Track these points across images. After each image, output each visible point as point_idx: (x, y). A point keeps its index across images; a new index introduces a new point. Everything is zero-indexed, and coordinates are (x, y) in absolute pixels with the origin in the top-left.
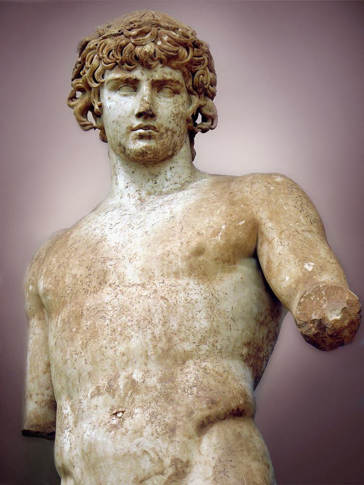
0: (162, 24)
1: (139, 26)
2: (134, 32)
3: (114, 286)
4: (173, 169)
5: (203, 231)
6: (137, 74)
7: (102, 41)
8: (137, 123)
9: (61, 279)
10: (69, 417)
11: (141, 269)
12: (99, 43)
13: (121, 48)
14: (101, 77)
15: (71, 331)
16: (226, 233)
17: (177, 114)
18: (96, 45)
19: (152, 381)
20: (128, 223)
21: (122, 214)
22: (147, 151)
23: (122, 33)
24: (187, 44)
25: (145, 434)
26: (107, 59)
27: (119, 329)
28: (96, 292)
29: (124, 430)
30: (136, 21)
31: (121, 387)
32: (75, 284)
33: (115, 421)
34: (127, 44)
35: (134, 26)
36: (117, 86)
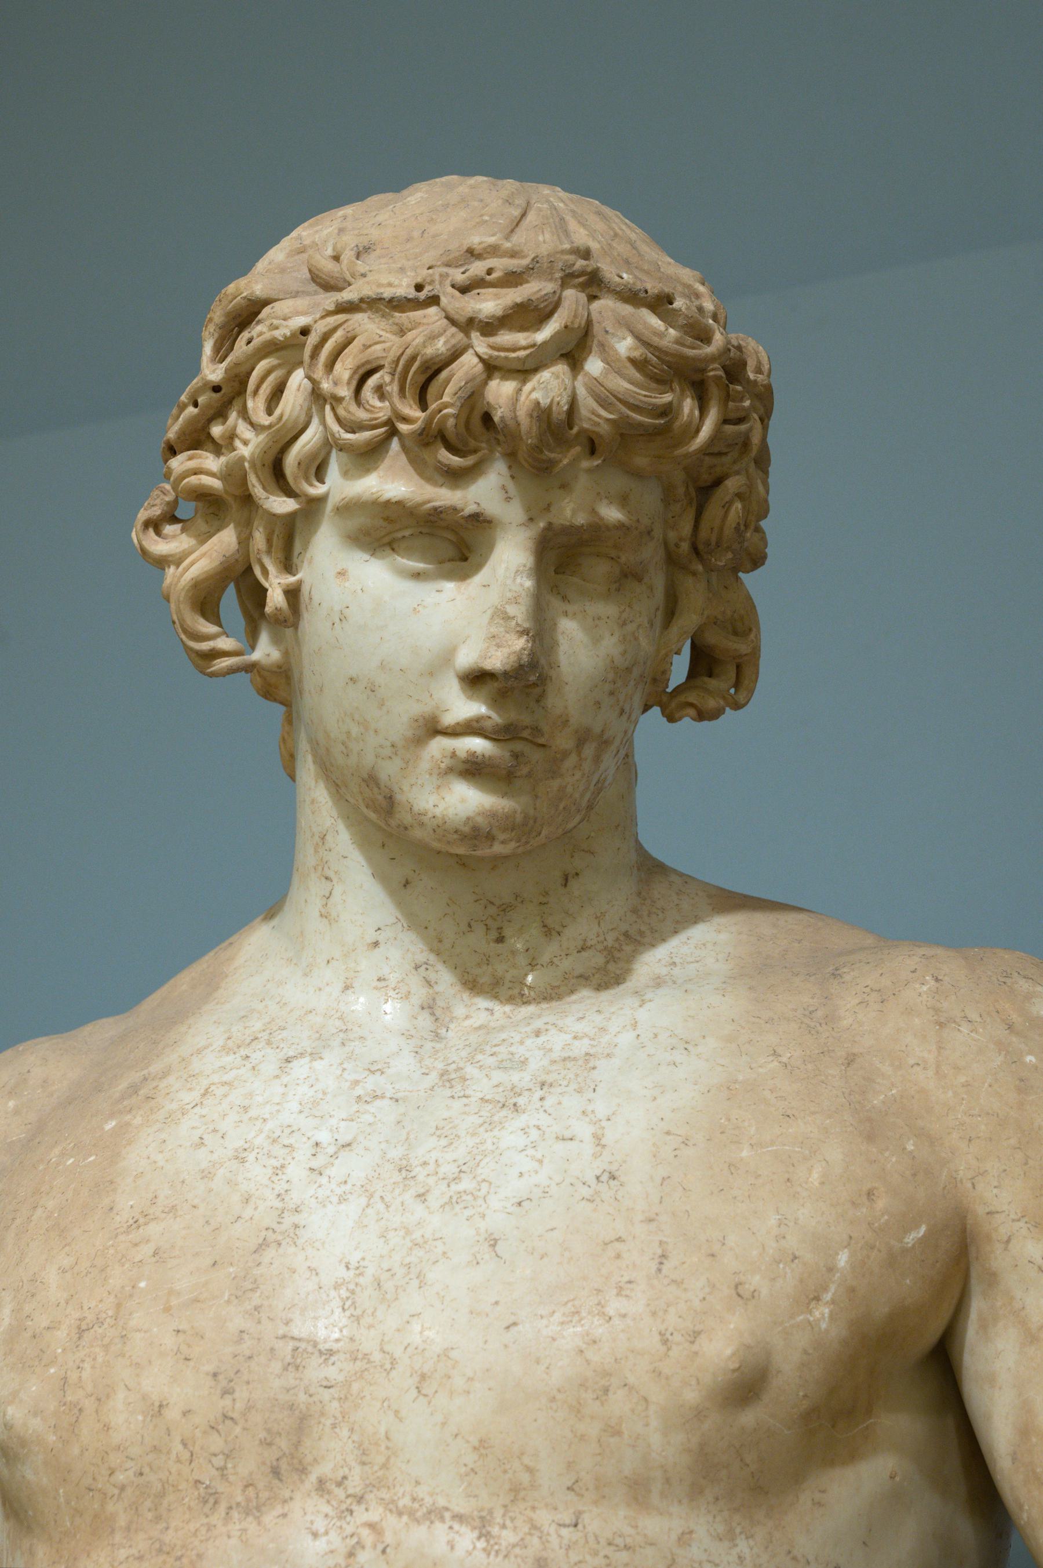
0: (609, 271)
1: (513, 279)
2: (488, 304)
3: (340, 1493)
4: (573, 884)
5: (757, 1278)
6: (488, 492)
7: (332, 320)
8: (463, 707)
9: (89, 1405)
11: (474, 1441)
12: (320, 328)
13: (423, 380)
14: (313, 471)
16: (852, 1290)
17: (629, 670)
18: (305, 332)
20: (395, 1153)
21: (359, 1091)
22: (495, 832)
23: (434, 300)
24: (704, 371)
26: (353, 408)
28: (254, 1509)
30: (493, 251)
32: (155, 1449)
34: (455, 355)
35: (489, 272)
36: (386, 530)
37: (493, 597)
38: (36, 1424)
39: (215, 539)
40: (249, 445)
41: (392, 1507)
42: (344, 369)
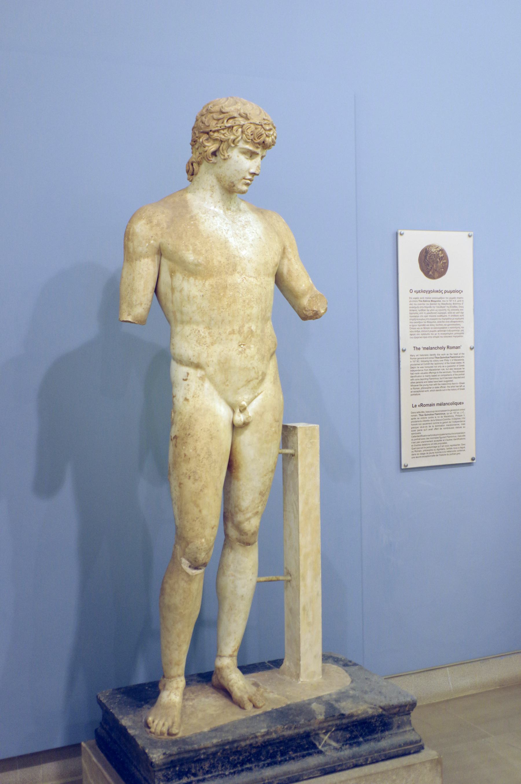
2: (267, 128)
6: (259, 151)
10: (207, 339)
12: (248, 125)
15: (219, 294)
19: (259, 332)
25: (255, 359)
27: (247, 301)
28: (232, 275)
29: (246, 356)
30: (267, 120)
31: (246, 332)
33: (240, 349)
36: (245, 152)
37: (257, 164)
38: (203, 262)
39: (215, 145)
40: (232, 137)
41: (246, 275)
42: (249, 131)
